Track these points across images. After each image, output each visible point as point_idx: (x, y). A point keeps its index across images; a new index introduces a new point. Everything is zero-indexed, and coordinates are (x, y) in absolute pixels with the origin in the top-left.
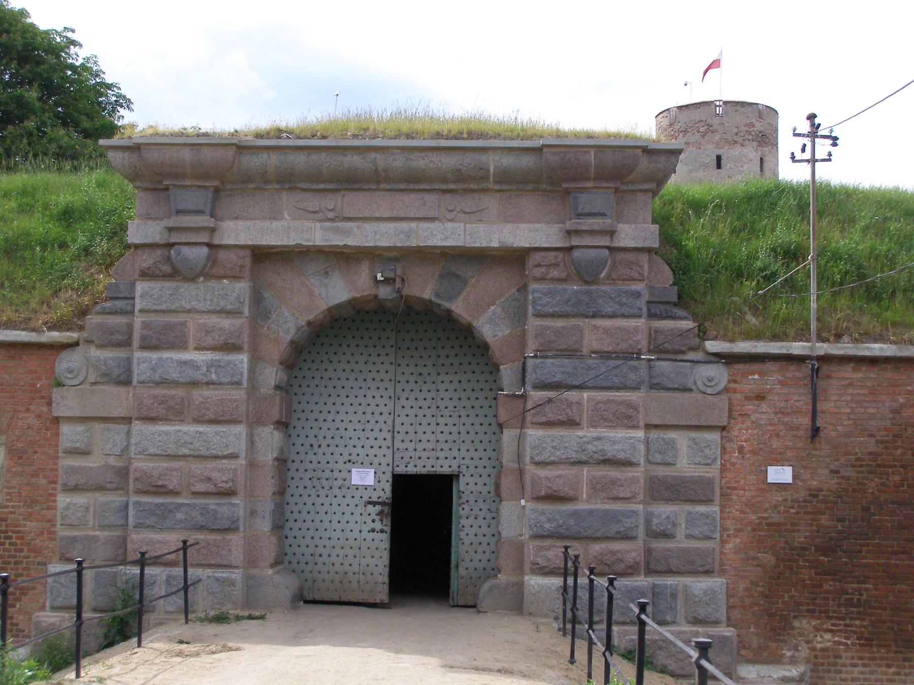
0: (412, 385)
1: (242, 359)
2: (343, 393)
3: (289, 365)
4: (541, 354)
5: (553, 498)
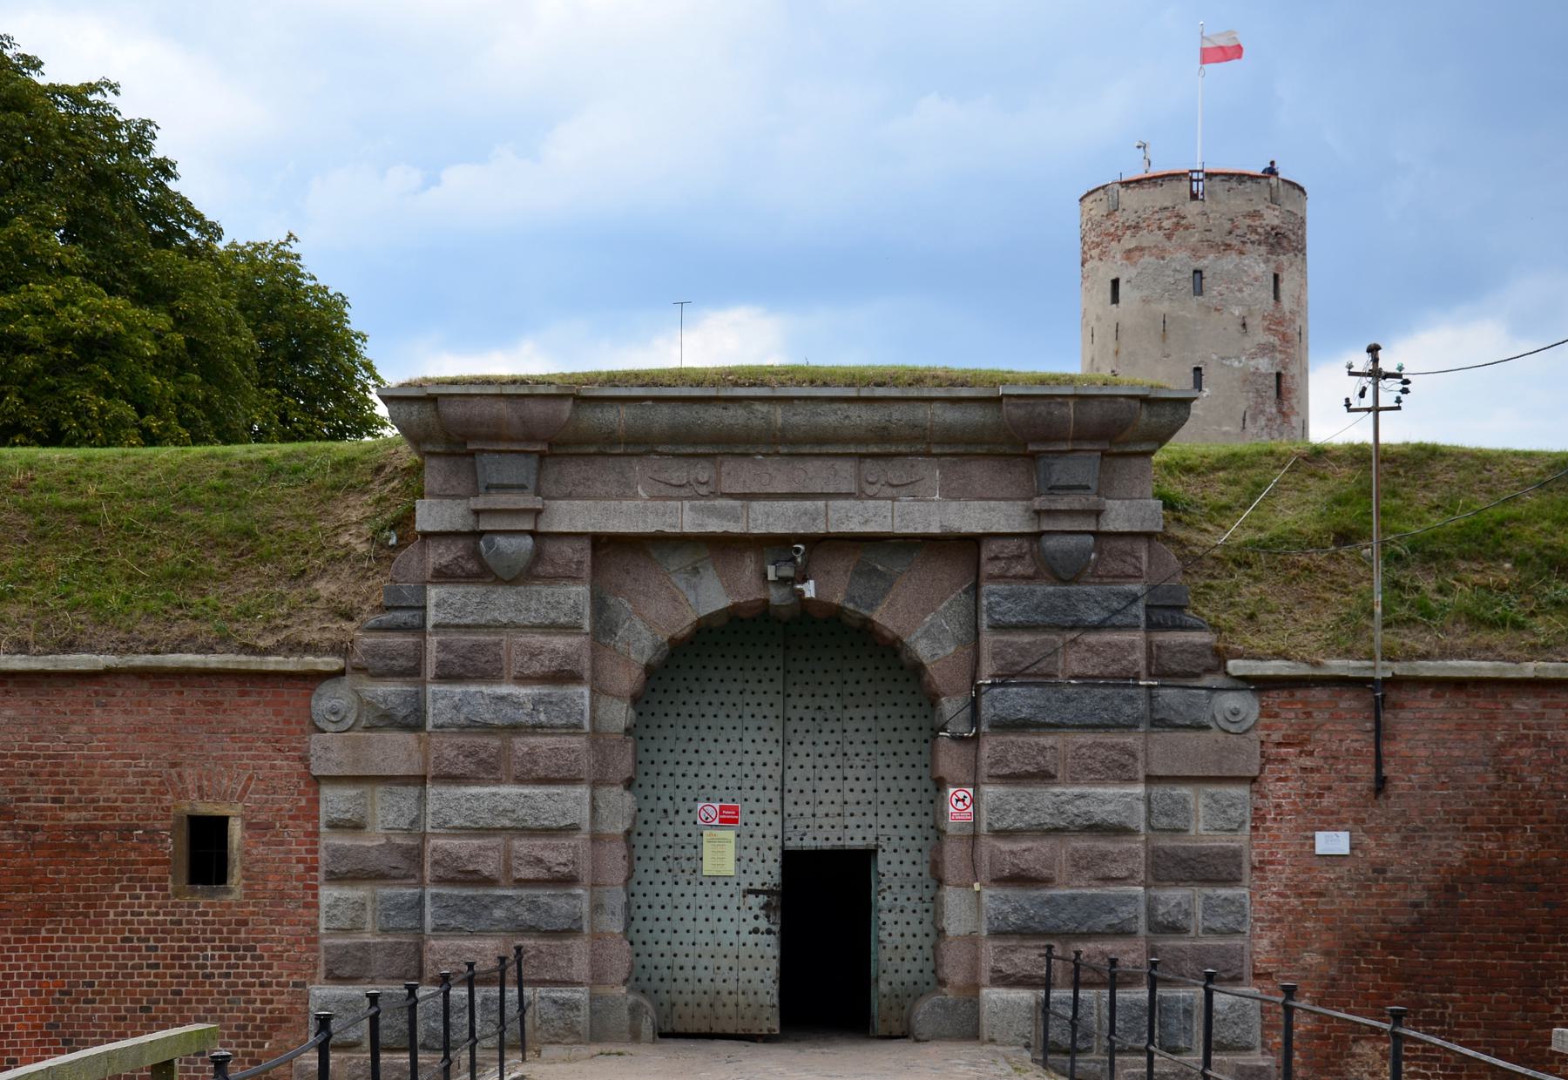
0: (808, 723)
1: (581, 694)
2: (709, 737)
3: (637, 700)
4: (1004, 680)
5: (1020, 879)
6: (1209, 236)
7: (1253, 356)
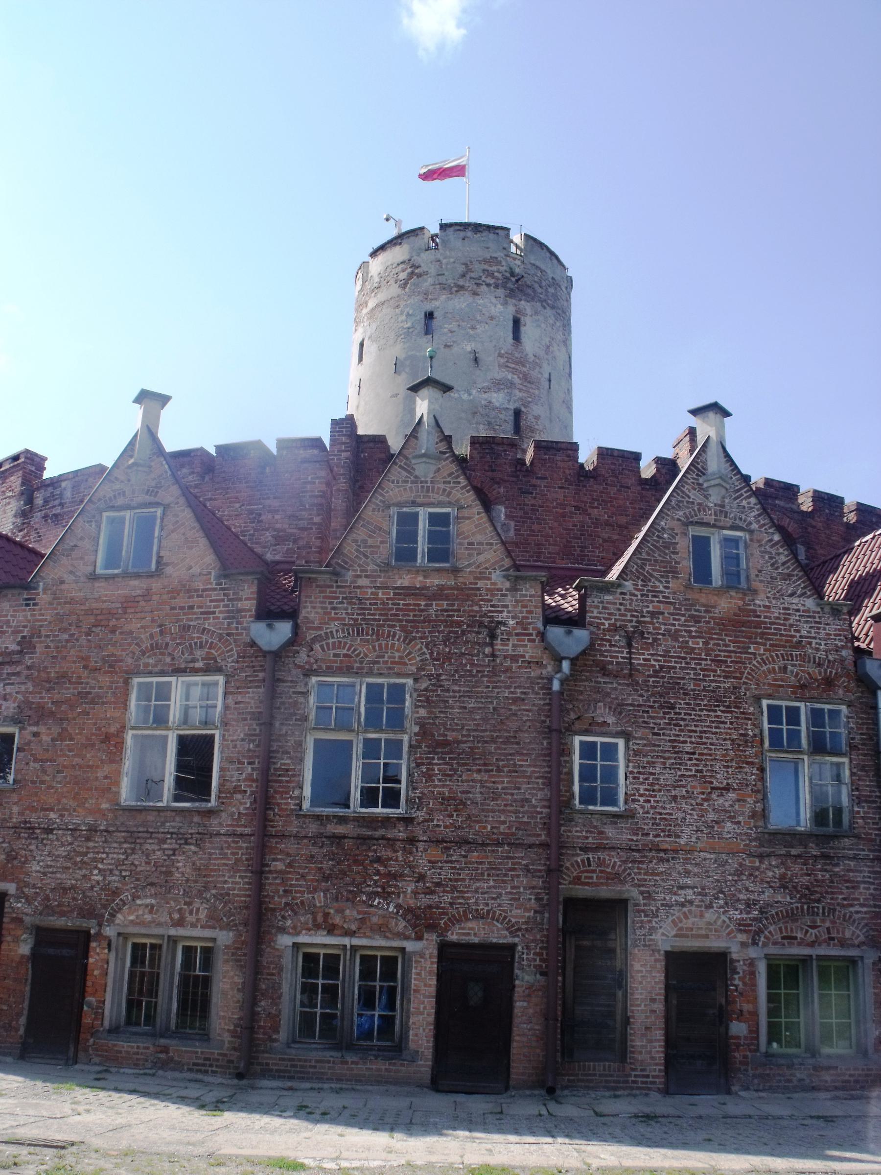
6: (442, 279)
7: (486, 390)
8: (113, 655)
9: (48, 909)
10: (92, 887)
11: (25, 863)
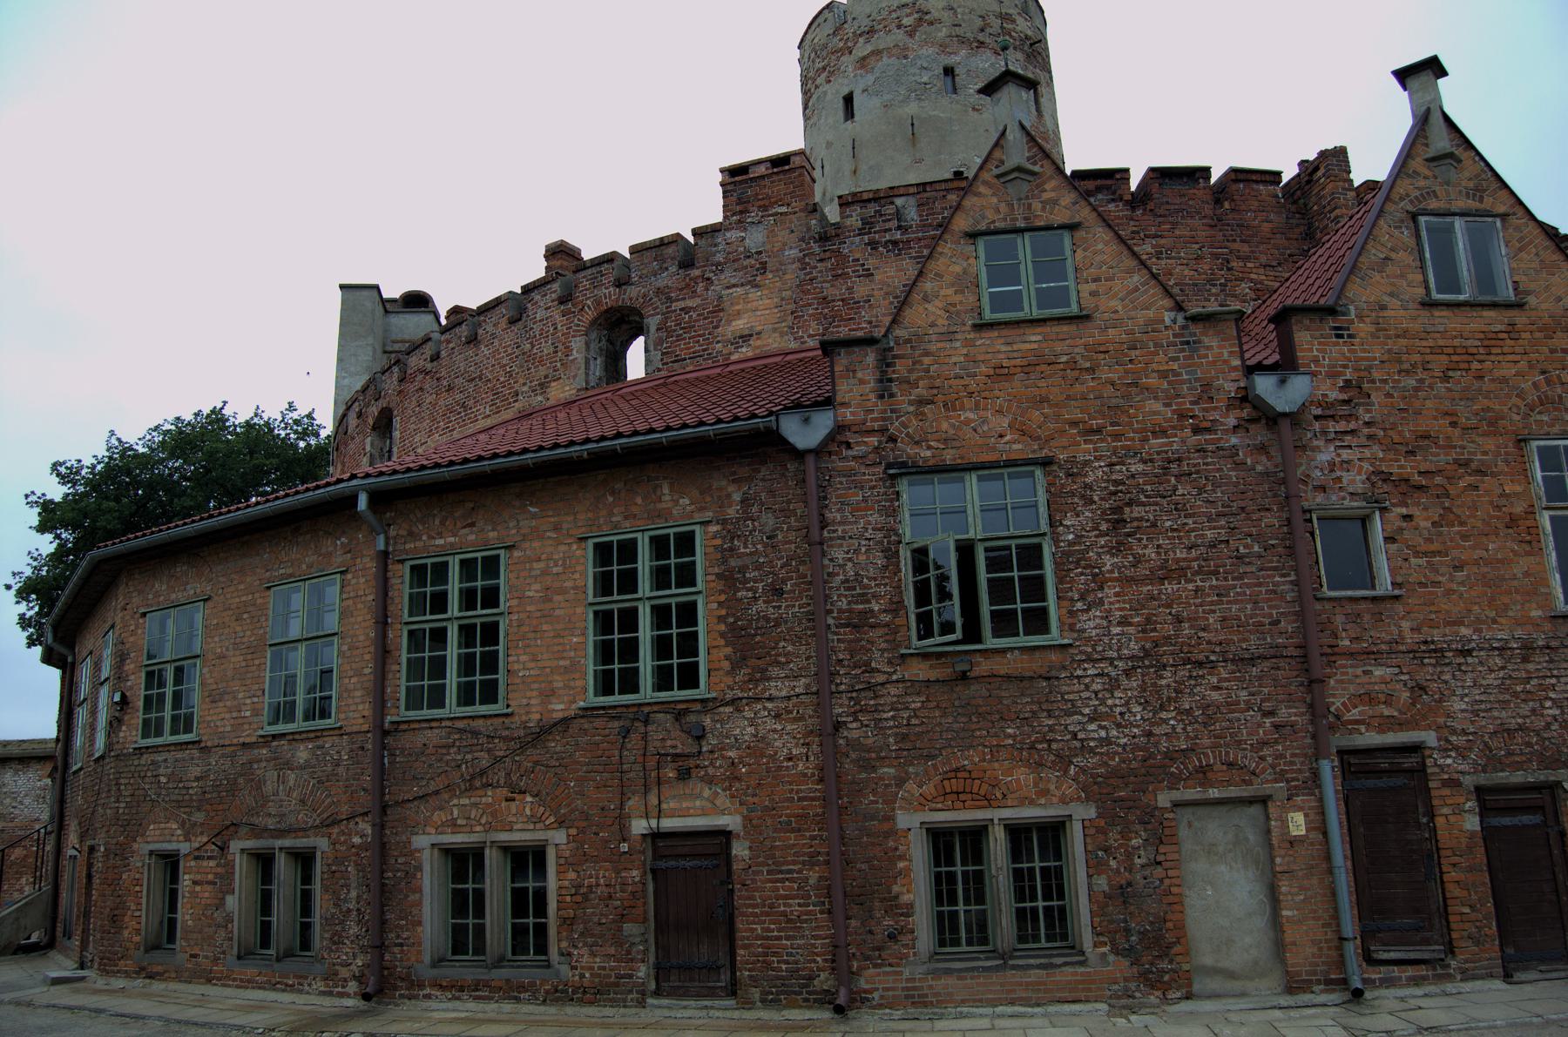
8: (1488, 409)
9: (1493, 762)
10: (1548, 725)
11: (1440, 701)
